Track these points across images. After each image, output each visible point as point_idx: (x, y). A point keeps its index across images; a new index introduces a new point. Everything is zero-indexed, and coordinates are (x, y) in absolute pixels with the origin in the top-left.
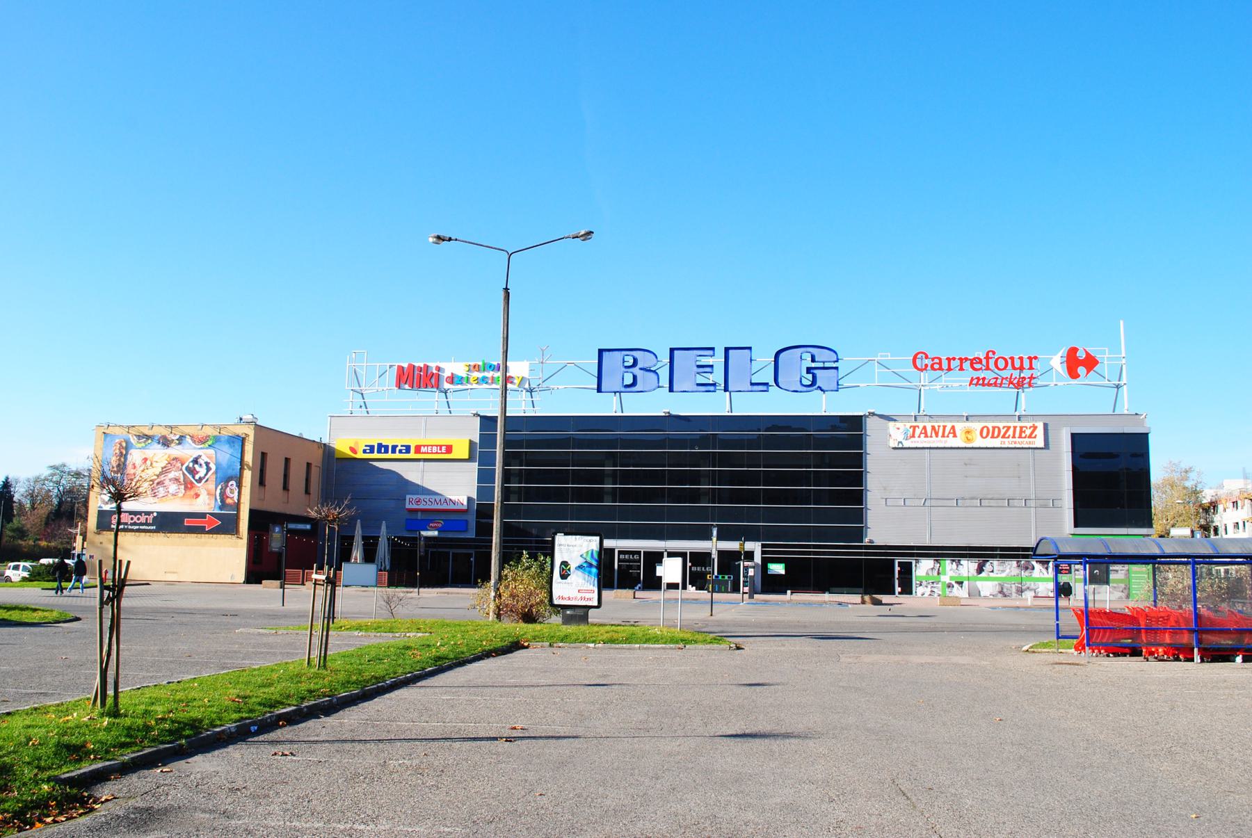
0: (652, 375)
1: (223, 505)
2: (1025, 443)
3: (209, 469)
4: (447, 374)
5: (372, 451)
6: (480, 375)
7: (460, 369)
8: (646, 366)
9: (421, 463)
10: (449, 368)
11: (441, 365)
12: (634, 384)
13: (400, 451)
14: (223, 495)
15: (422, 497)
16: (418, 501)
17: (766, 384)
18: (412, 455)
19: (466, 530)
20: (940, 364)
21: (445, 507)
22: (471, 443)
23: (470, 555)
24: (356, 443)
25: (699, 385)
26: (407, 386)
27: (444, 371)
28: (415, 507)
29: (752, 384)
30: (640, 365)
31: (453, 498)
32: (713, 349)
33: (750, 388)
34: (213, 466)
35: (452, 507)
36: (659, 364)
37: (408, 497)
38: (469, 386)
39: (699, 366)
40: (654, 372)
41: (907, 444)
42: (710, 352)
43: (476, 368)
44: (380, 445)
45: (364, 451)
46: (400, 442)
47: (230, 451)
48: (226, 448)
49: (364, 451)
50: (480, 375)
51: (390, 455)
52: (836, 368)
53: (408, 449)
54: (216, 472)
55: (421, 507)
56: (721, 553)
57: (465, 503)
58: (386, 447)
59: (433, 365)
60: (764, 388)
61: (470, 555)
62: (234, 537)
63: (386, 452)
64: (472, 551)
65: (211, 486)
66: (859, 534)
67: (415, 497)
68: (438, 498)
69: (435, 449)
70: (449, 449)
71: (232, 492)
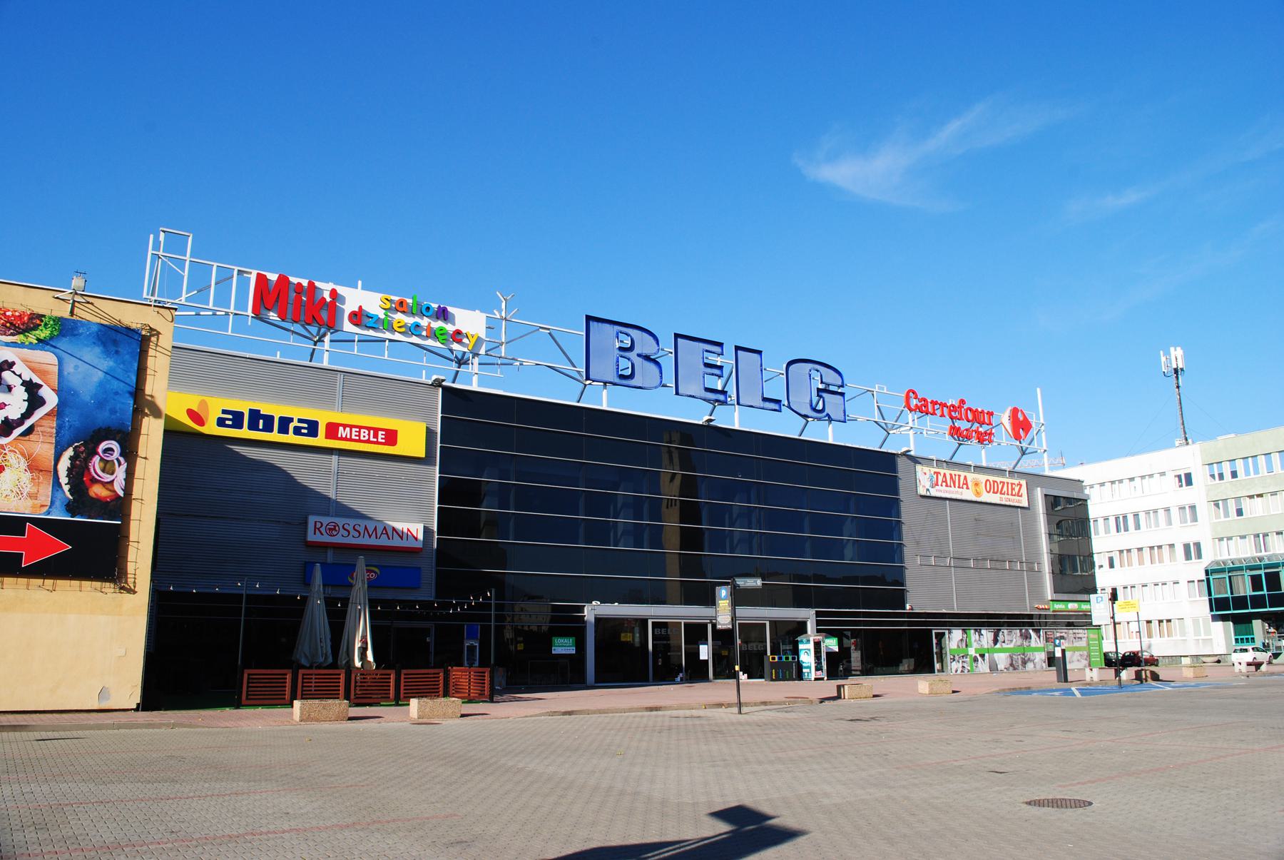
0: (652, 366)
1: (80, 499)
2: (1014, 501)
3: (35, 401)
4: (349, 307)
5: (237, 423)
6: (410, 320)
7: (373, 303)
8: (646, 352)
9: (335, 458)
10: (355, 298)
11: (341, 290)
12: (632, 376)
13: (297, 431)
14: (79, 474)
15: (340, 521)
16: (332, 530)
17: (778, 402)
18: (321, 440)
19: (416, 587)
20: (926, 406)
21: (383, 541)
22: (430, 433)
23: (426, 632)
24: (203, 404)
25: (707, 390)
26: (273, 316)
27: (343, 300)
28: (326, 538)
29: (765, 399)
30: (637, 350)
31: (399, 526)
32: (720, 345)
33: (762, 404)
34: (51, 399)
35: (396, 542)
36: (661, 353)
37: (312, 520)
38: (388, 335)
39: (707, 365)
40: (655, 362)
41: (934, 493)
42: (717, 349)
43: (401, 307)
44: (255, 415)
45: (221, 422)
46: (297, 412)
47: (107, 364)
48: (93, 354)
49: (221, 422)
50: (410, 320)
51: (274, 436)
52: (842, 394)
53: (312, 428)
54: (59, 412)
55: (338, 539)
56: (775, 624)
57: (421, 537)
58: (269, 420)
59: (325, 288)
60: (776, 407)
61: (426, 632)
62: (109, 587)
63: (268, 428)
64: (430, 625)
65: (43, 447)
66: (899, 598)
67: (325, 520)
68: (363, 523)
69: (364, 433)
70: (391, 437)
71: (108, 467)
